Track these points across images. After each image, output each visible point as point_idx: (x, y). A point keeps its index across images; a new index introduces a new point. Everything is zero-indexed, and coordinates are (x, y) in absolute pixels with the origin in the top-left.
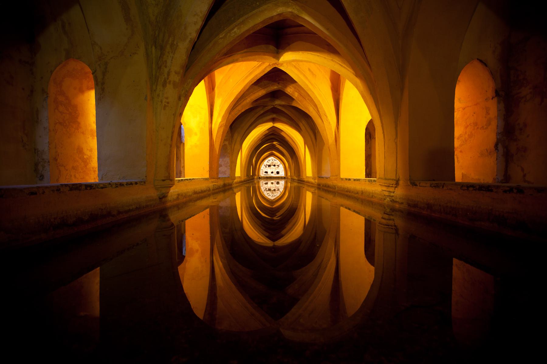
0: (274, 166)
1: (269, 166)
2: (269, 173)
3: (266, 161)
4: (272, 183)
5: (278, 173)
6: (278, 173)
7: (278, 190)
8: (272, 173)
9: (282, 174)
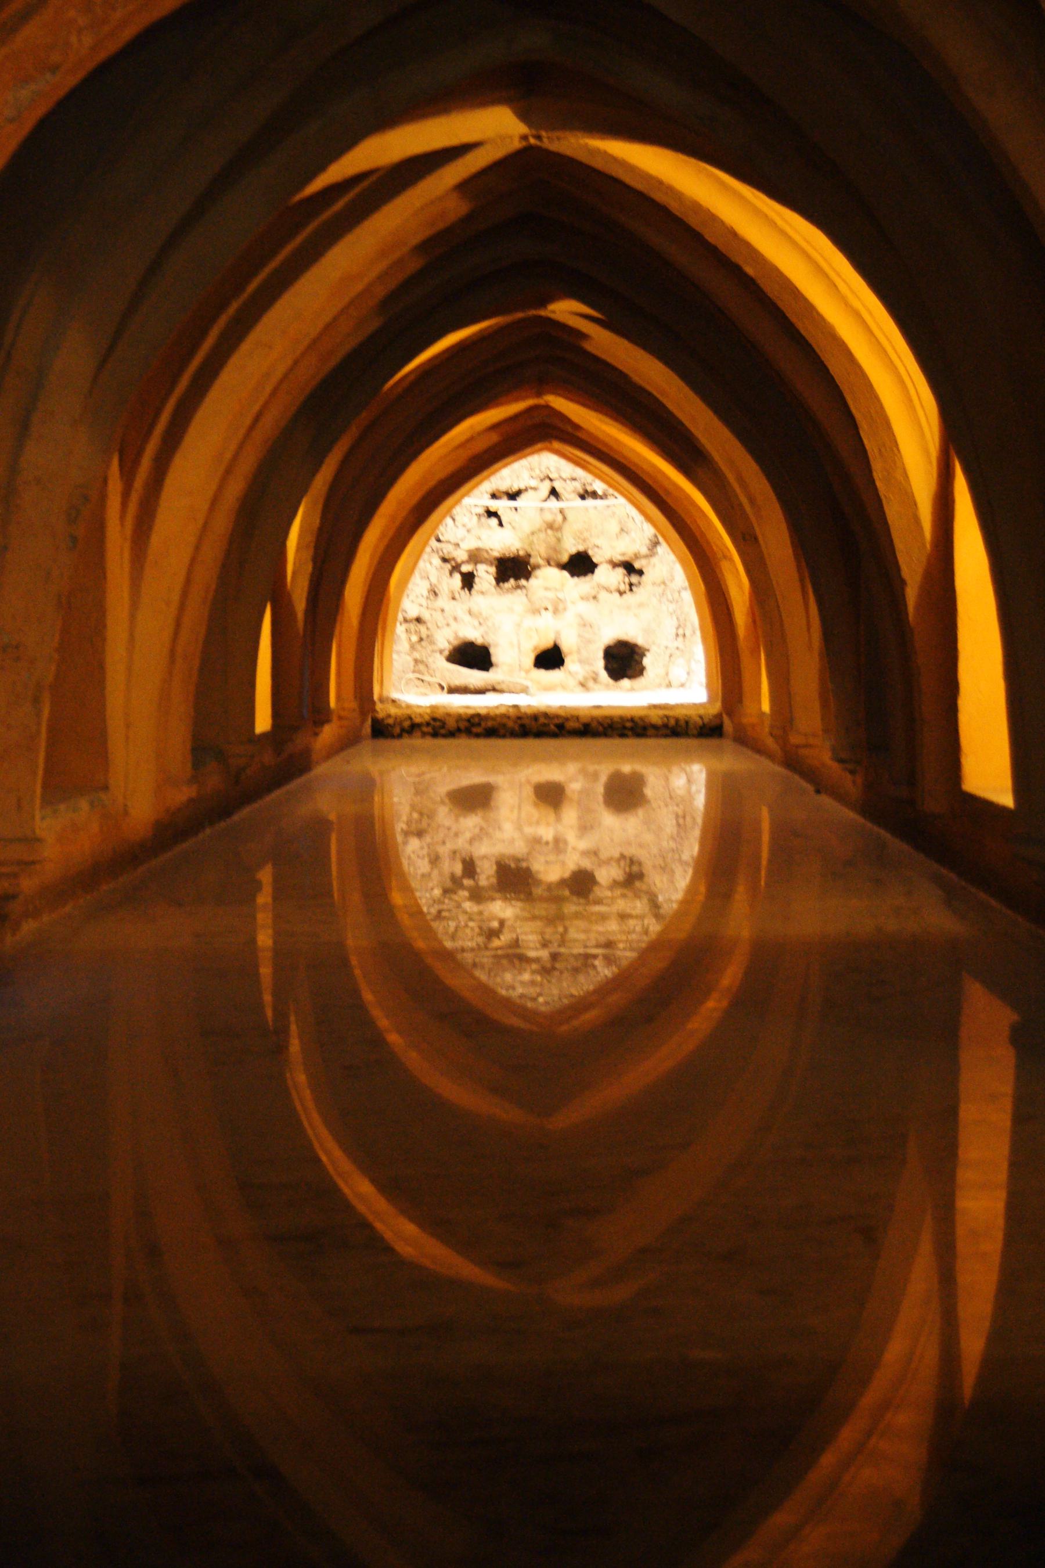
0: (580, 565)
1: (513, 569)
2: (512, 656)
3: (475, 498)
4: (551, 796)
5: (623, 660)
6: (623, 660)
7: (633, 878)
8: (550, 658)
9: (681, 677)
